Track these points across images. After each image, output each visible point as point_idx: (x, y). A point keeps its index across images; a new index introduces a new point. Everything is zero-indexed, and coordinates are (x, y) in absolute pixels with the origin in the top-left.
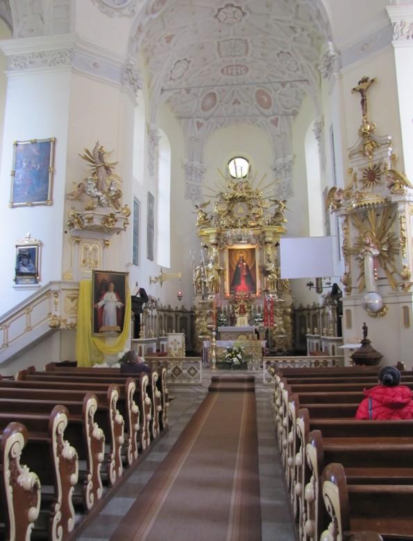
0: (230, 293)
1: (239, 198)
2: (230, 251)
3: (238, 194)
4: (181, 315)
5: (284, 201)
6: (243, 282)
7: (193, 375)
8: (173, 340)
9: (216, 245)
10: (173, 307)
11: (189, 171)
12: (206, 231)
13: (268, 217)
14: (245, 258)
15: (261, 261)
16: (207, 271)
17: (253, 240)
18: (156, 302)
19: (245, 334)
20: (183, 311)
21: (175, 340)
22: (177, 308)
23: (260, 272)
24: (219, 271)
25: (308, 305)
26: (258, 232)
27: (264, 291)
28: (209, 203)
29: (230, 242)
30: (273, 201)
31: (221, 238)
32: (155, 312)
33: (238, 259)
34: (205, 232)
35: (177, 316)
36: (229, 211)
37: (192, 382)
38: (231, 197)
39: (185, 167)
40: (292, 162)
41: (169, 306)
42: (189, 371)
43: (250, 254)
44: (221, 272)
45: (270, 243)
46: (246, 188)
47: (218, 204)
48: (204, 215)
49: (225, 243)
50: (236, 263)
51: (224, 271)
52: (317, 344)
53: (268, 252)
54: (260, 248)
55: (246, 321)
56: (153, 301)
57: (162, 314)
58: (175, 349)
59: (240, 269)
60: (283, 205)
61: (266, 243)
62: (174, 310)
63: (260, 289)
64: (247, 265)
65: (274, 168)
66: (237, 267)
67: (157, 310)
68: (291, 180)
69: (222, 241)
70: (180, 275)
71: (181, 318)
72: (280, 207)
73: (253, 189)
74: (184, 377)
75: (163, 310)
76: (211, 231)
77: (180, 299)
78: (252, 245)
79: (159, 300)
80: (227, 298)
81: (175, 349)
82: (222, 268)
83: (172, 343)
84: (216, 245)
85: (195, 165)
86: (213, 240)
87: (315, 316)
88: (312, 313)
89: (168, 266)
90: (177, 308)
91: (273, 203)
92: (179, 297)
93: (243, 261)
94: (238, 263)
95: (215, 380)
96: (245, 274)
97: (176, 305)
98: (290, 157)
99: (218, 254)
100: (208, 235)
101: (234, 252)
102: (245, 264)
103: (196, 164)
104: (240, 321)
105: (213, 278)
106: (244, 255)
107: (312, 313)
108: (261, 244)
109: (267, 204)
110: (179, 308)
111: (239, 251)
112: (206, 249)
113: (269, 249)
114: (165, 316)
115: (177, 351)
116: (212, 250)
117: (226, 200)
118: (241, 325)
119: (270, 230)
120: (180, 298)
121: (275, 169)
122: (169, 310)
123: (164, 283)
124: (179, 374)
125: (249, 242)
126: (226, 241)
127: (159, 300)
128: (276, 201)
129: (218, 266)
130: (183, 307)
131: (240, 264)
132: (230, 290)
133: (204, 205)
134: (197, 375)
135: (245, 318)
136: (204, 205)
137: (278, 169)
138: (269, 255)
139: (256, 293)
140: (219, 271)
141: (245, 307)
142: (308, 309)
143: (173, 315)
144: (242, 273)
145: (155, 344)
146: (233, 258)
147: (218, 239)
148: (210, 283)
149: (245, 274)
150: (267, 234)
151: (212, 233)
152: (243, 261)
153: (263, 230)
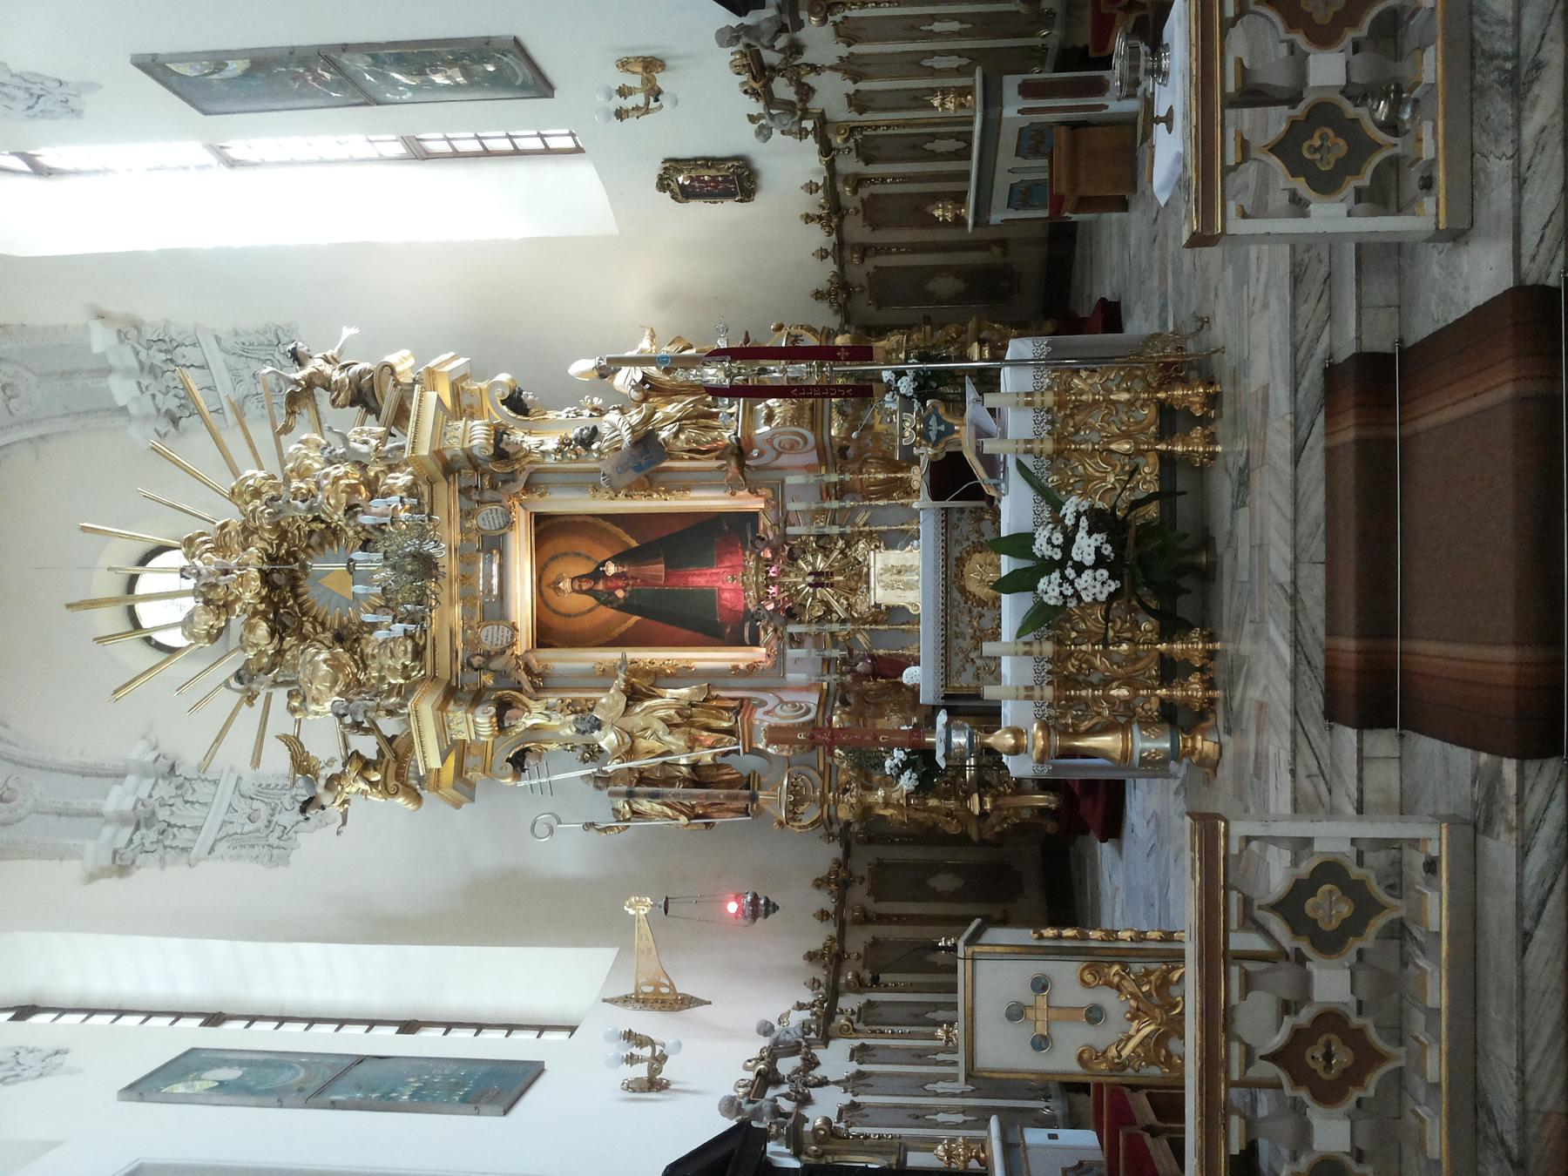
0: (755, 642)
1: (281, 591)
2: (545, 636)
3: (251, 592)
4: (859, 894)
5: (297, 358)
6: (700, 579)
7: (1366, 906)
8: (1021, 1033)
9: (503, 707)
10: (819, 936)
11: (152, 835)
12: (429, 756)
13: (364, 434)
14: (584, 568)
15: (589, 482)
16: (631, 753)
17: (487, 518)
18: (774, 1053)
19: (961, 561)
20: (838, 881)
21: (1016, 1013)
22: (823, 915)
23: (648, 484)
24: (634, 695)
25: (823, 254)
26: (447, 498)
27: (741, 466)
28: (293, 743)
29: (491, 636)
30: (291, 413)
31: (472, 680)
32: (835, 1059)
33: (589, 601)
34: (434, 762)
35: (866, 919)
36: (339, 638)
37: (1437, 911)
38: (263, 629)
39: (121, 867)
40: (128, 329)
41: (811, 957)
42: (1329, 944)
43: (562, 544)
44: (641, 683)
45: (499, 434)
46: (221, 547)
47: (299, 697)
48: (352, 771)
49: (496, 664)
50: (606, 613)
51: (634, 671)
52: (1026, 90)
53: (551, 444)
54: (529, 487)
55: (894, 557)
56: (767, 1078)
57: (849, 1002)
58: (1094, 1015)
59: (632, 595)
60: (315, 364)
61: (501, 455)
62: (831, 929)
63: (733, 488)
64: (616, 559)
65: (164, 426)
66: (627, 607)
67: (826, 1039)
68: (218, 340)
69: (488, 679)
70: (640, 908)
71: (878, 894)
72: (327, 385)
73: (233, 516)
74: (1388, 988)
75: (834, 993)
76: (428, 728)
77: (771, 908)
78: (509, 524)
79: (766, 1030)
80: (779, 660)
81: (1094, 1015)
82: (620, 682)
83: (1041, 1043)
84: (503, 707)
85: (127, 805)
86: (477, 724)
87: (874, 211)
88: (856, 230)
89: (605, 956)
90: (823, 915)
91: (306, 414)
92: (755, 915)
93: (597, 575)
94: (606, 600)
95: (1370, 694)
96: (659, 569)
97: (802, 928)
98: (101, 340)
99: (553, 699)
100: (458, 750)
101: (557, 622)
102: (611, 569)
103: (119, 798)
104: (888, 586)
105: (671, 726)
106: (569, 571)
107: (856, 230)
108: (511, 478)
109: (303, 443)
110: (825, 901)
111: (549, 593)
112: (530, 761)
113: (530, 442)
114: (859, 986)
115: (1108, 999)
116: (535, 728)
117: (280, 652)
118: (908, 586)
119: (422, 436)
120: (760, 909)
121: (175, 421)
122: (831, 958)
123: (684, 988)
124: (1355, 1039)
125: (495, 544)
126: (488, 656)
127: (766, 1030)
128: (293, 399)
129: (610, 701)
130: (819, 883)
131: (611, 593)
132: (740, 643)
133: (302, 764)
134: (1369, 874)
135: (880, 561)
136: (302, 764)
137: (172, 403)
138: (564, 443)
139: (753, 517)
140: (634, 695)
141: (821, 564)
142: (840, 250)
143: (858, 940)
144: (653, 576)
145: (1035, 1137)
146: (586, 623)
147: (477, 698)
148: (693, 743)
149: (659, 569)
150: (454, 446)
151: (443, 728)
152: (597, 575)
153: (435, 468)
